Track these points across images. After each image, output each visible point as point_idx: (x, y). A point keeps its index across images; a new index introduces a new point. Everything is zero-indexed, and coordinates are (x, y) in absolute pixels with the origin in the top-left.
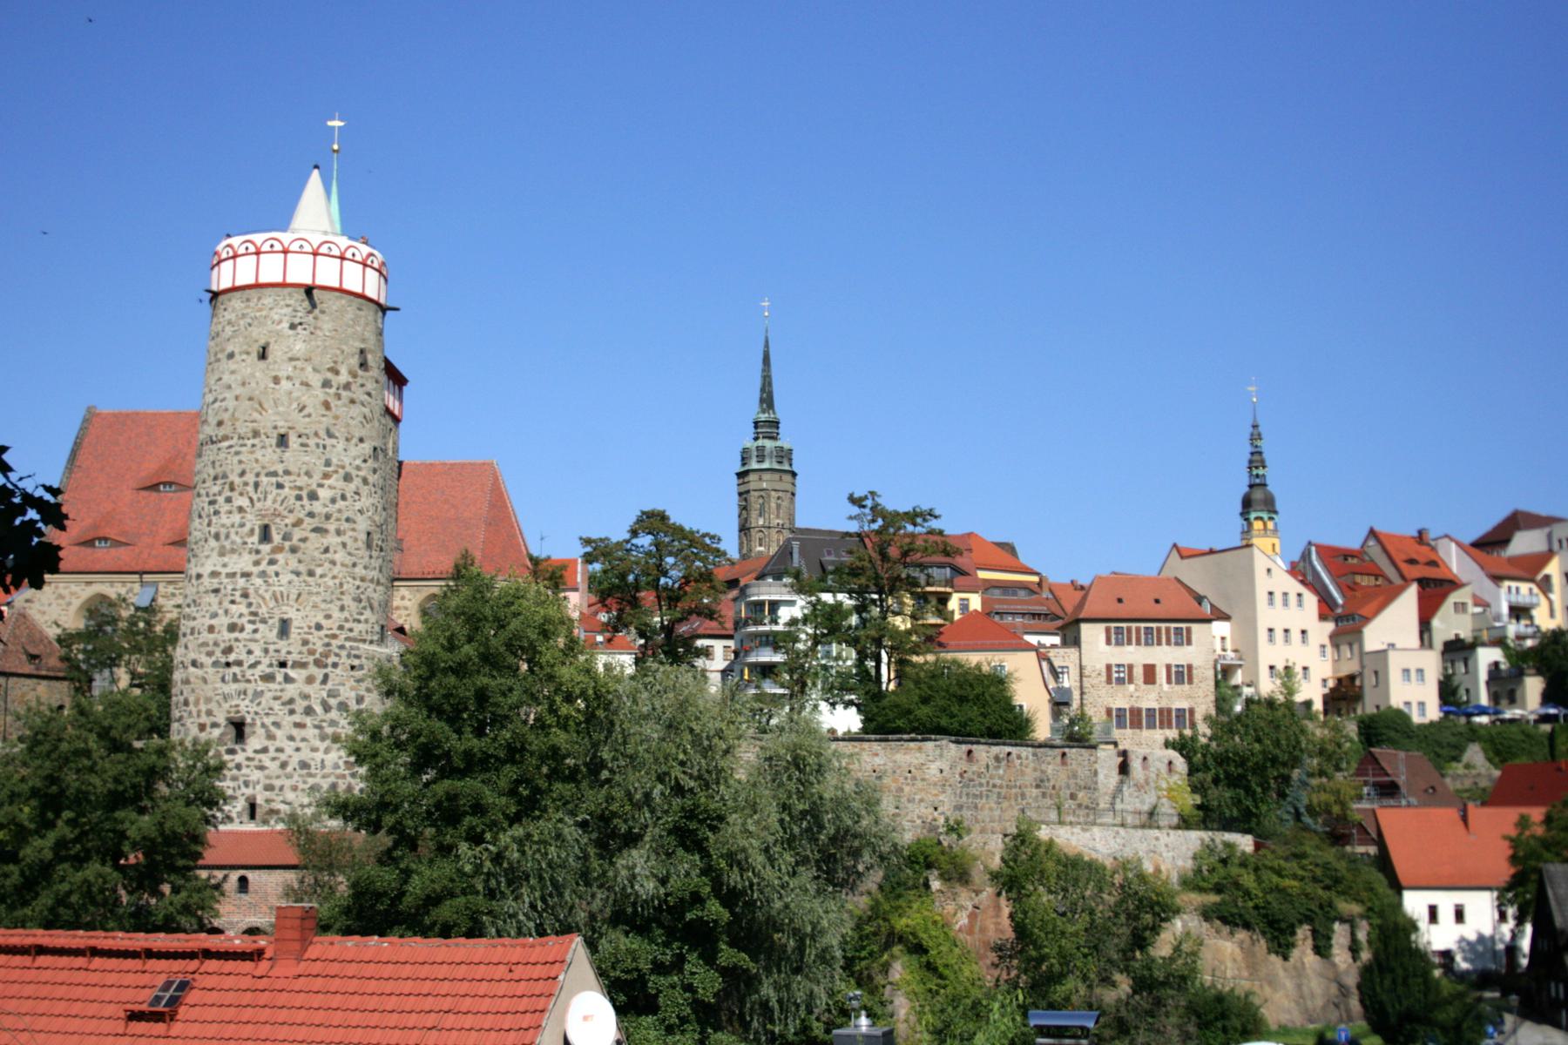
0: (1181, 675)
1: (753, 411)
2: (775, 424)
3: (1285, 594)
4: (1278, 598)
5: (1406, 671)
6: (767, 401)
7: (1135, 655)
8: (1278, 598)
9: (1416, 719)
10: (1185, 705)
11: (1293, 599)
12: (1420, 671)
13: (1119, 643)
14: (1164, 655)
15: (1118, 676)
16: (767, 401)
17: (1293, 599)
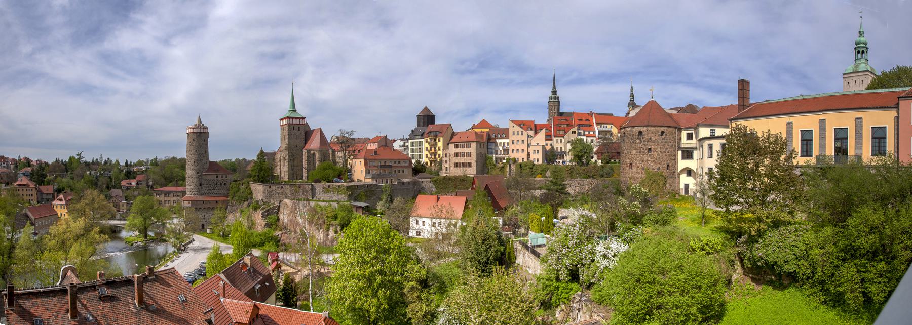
0: (469, 155)
1: (551, 89)
2: (556, 92)
3: (518, 132)
4: (516, 133)
5: (534, 151)
6: (554, 87)
7: (459, 150)
8: (516, 133)
9: (536, 163)
10: (470, 162)
11: (520, 133)
12: (538, 151)
13: (457, 148)
14: (466, 150)
15: (456, 155)
16: (554, 87)
17: (520, 133)
